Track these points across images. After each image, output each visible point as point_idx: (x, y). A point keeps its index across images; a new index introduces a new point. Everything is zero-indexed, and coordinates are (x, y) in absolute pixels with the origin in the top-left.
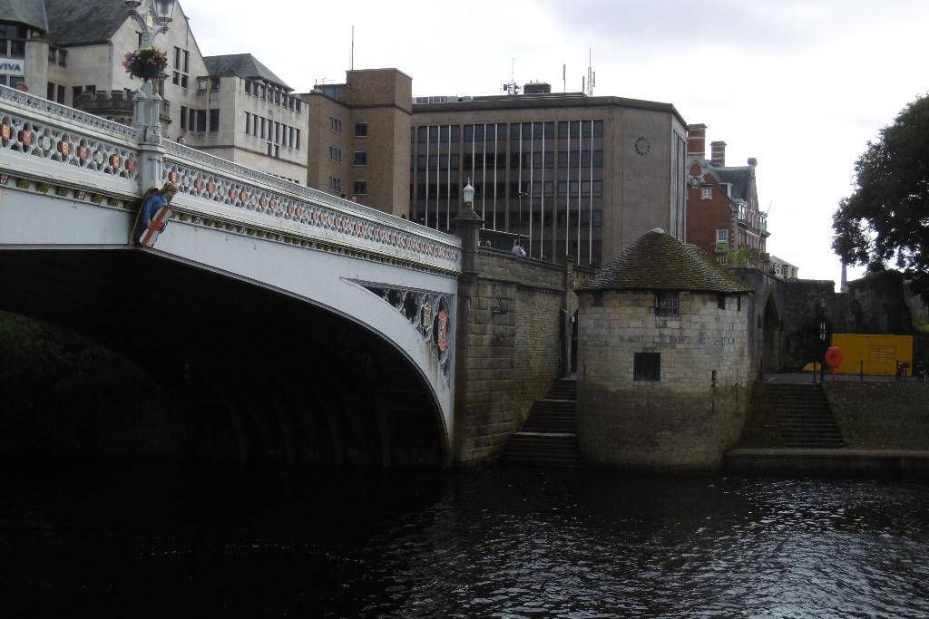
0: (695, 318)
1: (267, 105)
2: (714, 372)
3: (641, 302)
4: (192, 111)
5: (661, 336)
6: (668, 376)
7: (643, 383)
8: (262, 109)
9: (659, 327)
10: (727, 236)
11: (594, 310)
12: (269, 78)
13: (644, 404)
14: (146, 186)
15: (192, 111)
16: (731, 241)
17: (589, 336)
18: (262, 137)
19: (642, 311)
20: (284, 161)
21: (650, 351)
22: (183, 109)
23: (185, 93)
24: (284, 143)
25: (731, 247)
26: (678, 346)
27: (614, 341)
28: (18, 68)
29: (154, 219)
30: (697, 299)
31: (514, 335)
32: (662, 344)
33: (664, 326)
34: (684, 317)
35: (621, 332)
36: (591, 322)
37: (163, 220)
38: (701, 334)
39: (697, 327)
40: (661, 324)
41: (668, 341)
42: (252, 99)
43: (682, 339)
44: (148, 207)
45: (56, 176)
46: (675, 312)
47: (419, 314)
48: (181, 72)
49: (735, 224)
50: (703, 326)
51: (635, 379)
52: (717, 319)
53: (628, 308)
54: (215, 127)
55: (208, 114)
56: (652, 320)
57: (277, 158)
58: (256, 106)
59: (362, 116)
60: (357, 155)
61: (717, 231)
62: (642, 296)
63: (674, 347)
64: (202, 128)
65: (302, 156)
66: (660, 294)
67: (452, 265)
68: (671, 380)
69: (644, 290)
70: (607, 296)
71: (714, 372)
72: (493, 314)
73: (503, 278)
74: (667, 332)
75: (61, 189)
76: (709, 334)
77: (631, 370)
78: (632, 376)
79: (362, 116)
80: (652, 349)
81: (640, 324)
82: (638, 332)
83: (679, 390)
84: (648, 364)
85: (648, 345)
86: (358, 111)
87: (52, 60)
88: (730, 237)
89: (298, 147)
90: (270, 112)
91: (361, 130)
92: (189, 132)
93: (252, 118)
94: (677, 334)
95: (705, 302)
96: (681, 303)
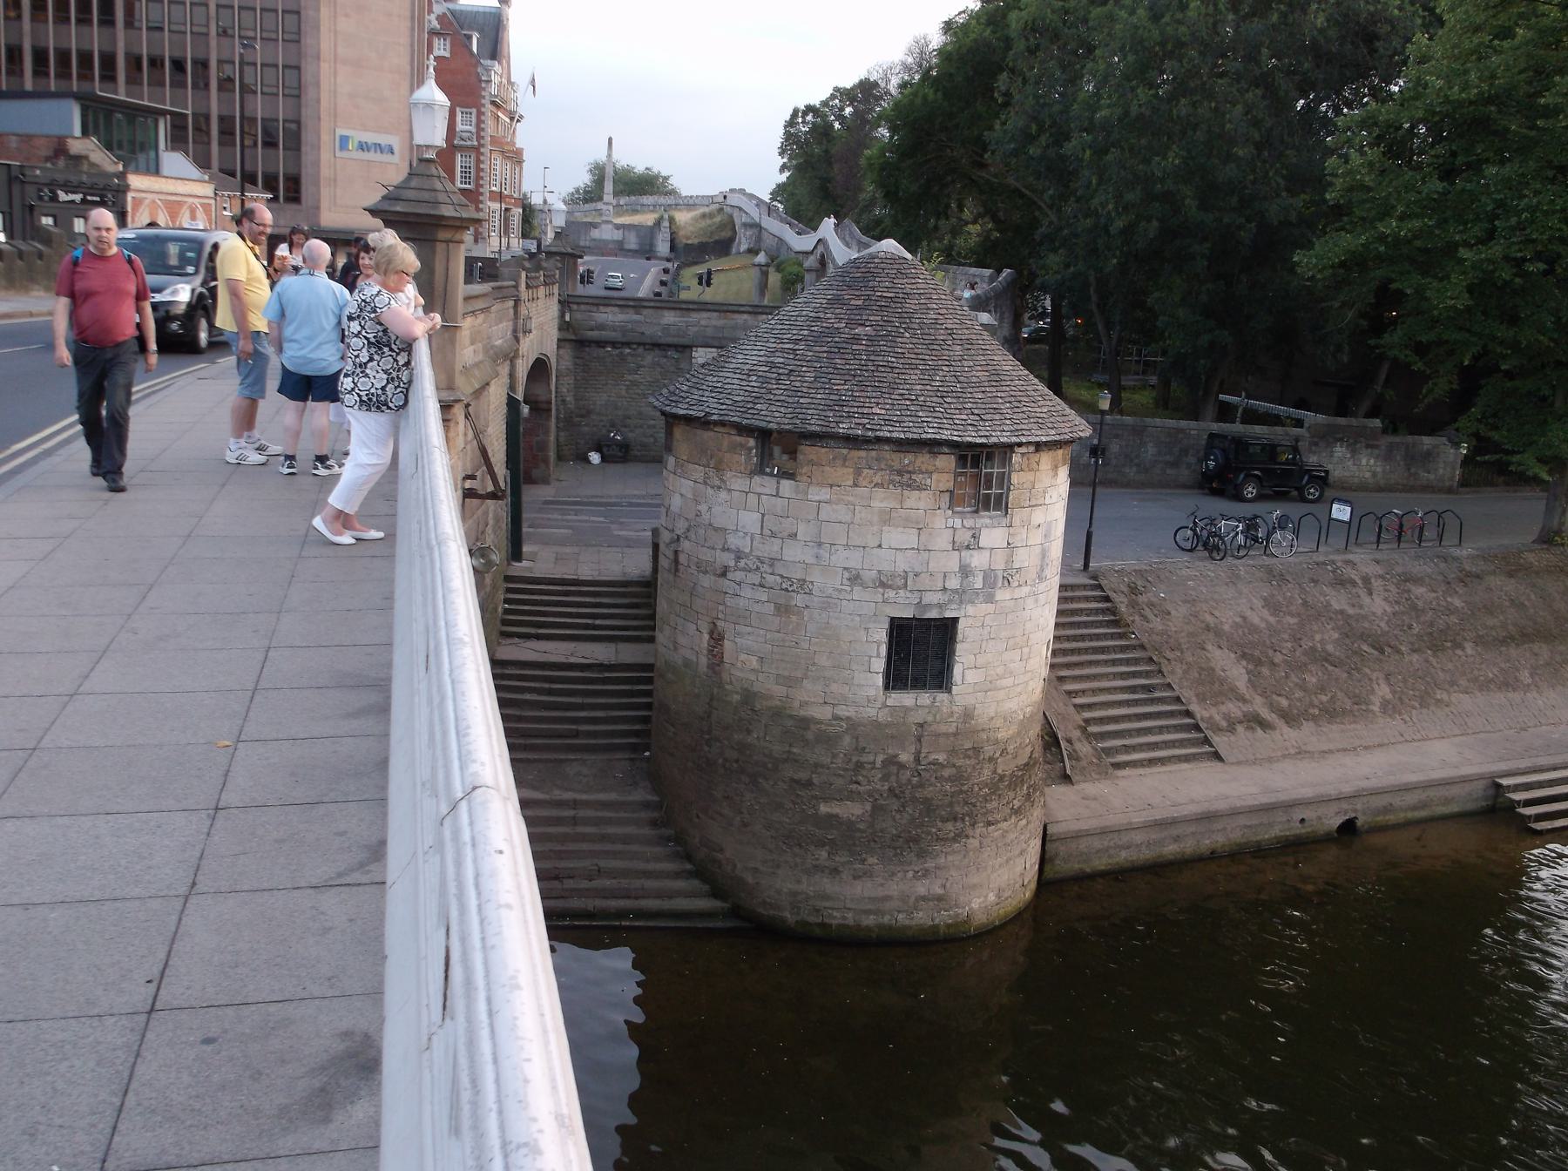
3: (918, 478)
5: (965, 571)
6: (972, 677)
9: (956, 547)
10: (474, 119)
11: (765, 484)
16: (479, 129)
17: (739, 555)
19: (918, 501)
21: (933, 614)
25: (479, 138)
32: (962, 596)
33: (974, 544)
34: (1018, 516)
35: (854, 560)
36: (750, 520)
40: (964, 537)
41: (979, 584)
49: (486, 102)
56: (946, 525)
62: (923, 460)
63: (990, 599)
70: (808, 452)
74: (978, 560)
77: (880, 665)
80: (940, 606)
81: (909, 538)
82: (902, 566)
85: (930, 598)
88: (479, 122)
94: (999, 565)
96: (1015, 478)
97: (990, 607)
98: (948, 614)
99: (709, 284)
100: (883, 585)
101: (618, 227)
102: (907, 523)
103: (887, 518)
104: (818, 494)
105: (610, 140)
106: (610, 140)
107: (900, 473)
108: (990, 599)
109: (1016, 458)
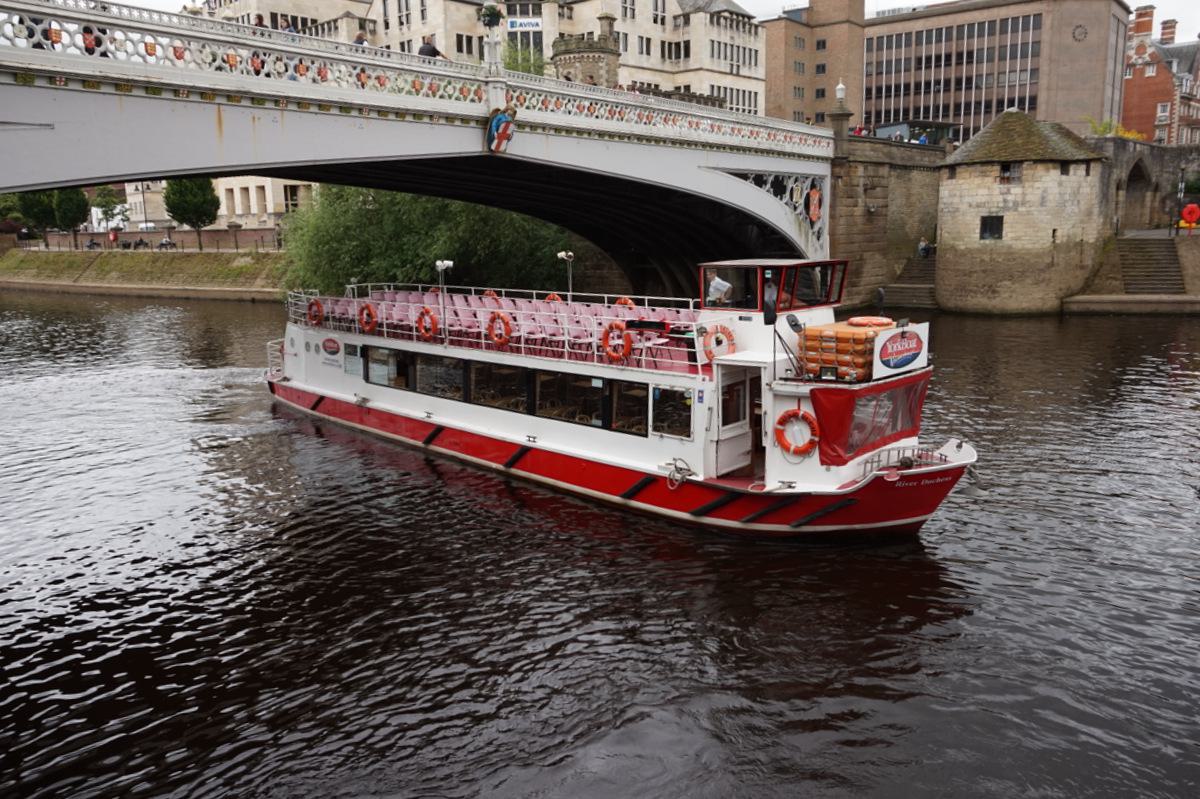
0: (1037, 185)
1: (729, 32)
2: (1054, 231)
4: (670, 44)
5: (1005, 201)
6: (1010, 235)
7: (987, 242)
8: (725, 36)
9: (1002, 194)
11: (950, 181)
12: (733, 10)
13: (986, 258)
14: (493, 107)
15: (670, 44)
18: (725, 58)
19: (989, 180)
20: (744, 77)
22: (663, 43)
23: (664, 30)
24: (744, 63)
26: (1020, 209)
27: (964, 207)
28: (537, 25)
29: (501, 130)
30: (1040, 168)
31: (887, 206)
32: (1006, 208)
34: (1027, 184)
36: (946, 193)
37: (509, 132)
38: (1043, 198)
39: (1040, 192)
41: (1011, 205)
42: (716, 28)
43: (1023, 204)
44: (494, 124)
45: (410, 107)
46: (1019, 180)
47: (788, 193)
48: (659, 13)
50: (1045, 191)
51: (982, 237)
52: (1060, 184)
54: (687, 55)
55: (682, 45)
56: (997, 187)
57: (738, 75)
58: (720, 35)
59: (820, 33)
60: (818, 67)
61: (1159, 105)
62: (989, 168)
63: (1016, 210)
64: (678, 56)
65: (760, 72)
66: (1006, 166)
67: (828, 151)
68: (1012, 239)
69: (991, 163)
70: (959, 170)
71: (1054, 231)
72: (865, 190)
73: (875, 160)
75: (418, 115)
76: (1050, 197)
77: (978, 231)
78: (978, 236)
79: (820, 33)
81: (986, 192)
82: (984, 200)
83: (1020, 246)
84: (992, 225)
85: (994, 210)
86: (818, 29)
87: (561, 15)
88: (1172, 109)
89: (756, 64)
90: (732, 38)
91: (821, 45)
92: (668, 61)
93: (716, 45)
94: (1019, 199)
95: (1048, 170)
103: (979, 186)
104: (961, 182)
108: (1016, 210)
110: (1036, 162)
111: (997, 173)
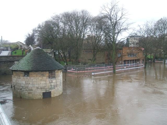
3: (44, 75)
5: (51, 86)
11: (25, 78)
17: (23, 87)
19: (45, 78)
21: (48, 91)
34: (57, 78)
35: (37, 86)
36: (24, 82)
41: (53, 87)
53: (40, 77)
56: (48, 80)
62: (45, 73)
63: (55, 89)
70: (30, 73)
74: (52, 84)
80: (49, 90)
81: (44, 82)
82: (44, 85)
85: (47, 89)
97: (54, 90)
98: (50, 91)
99: (16, 53)
100: (41, 89)
101: (3, 47)
102: (44, 80)
103: (41, 80)
104: (32, 78)
105: (2, 36)
106: (2, 36)
107: (42, 75)
108: (55, 89)
109: (56, 71)
110: (58, 70)
111: (48, 75)
